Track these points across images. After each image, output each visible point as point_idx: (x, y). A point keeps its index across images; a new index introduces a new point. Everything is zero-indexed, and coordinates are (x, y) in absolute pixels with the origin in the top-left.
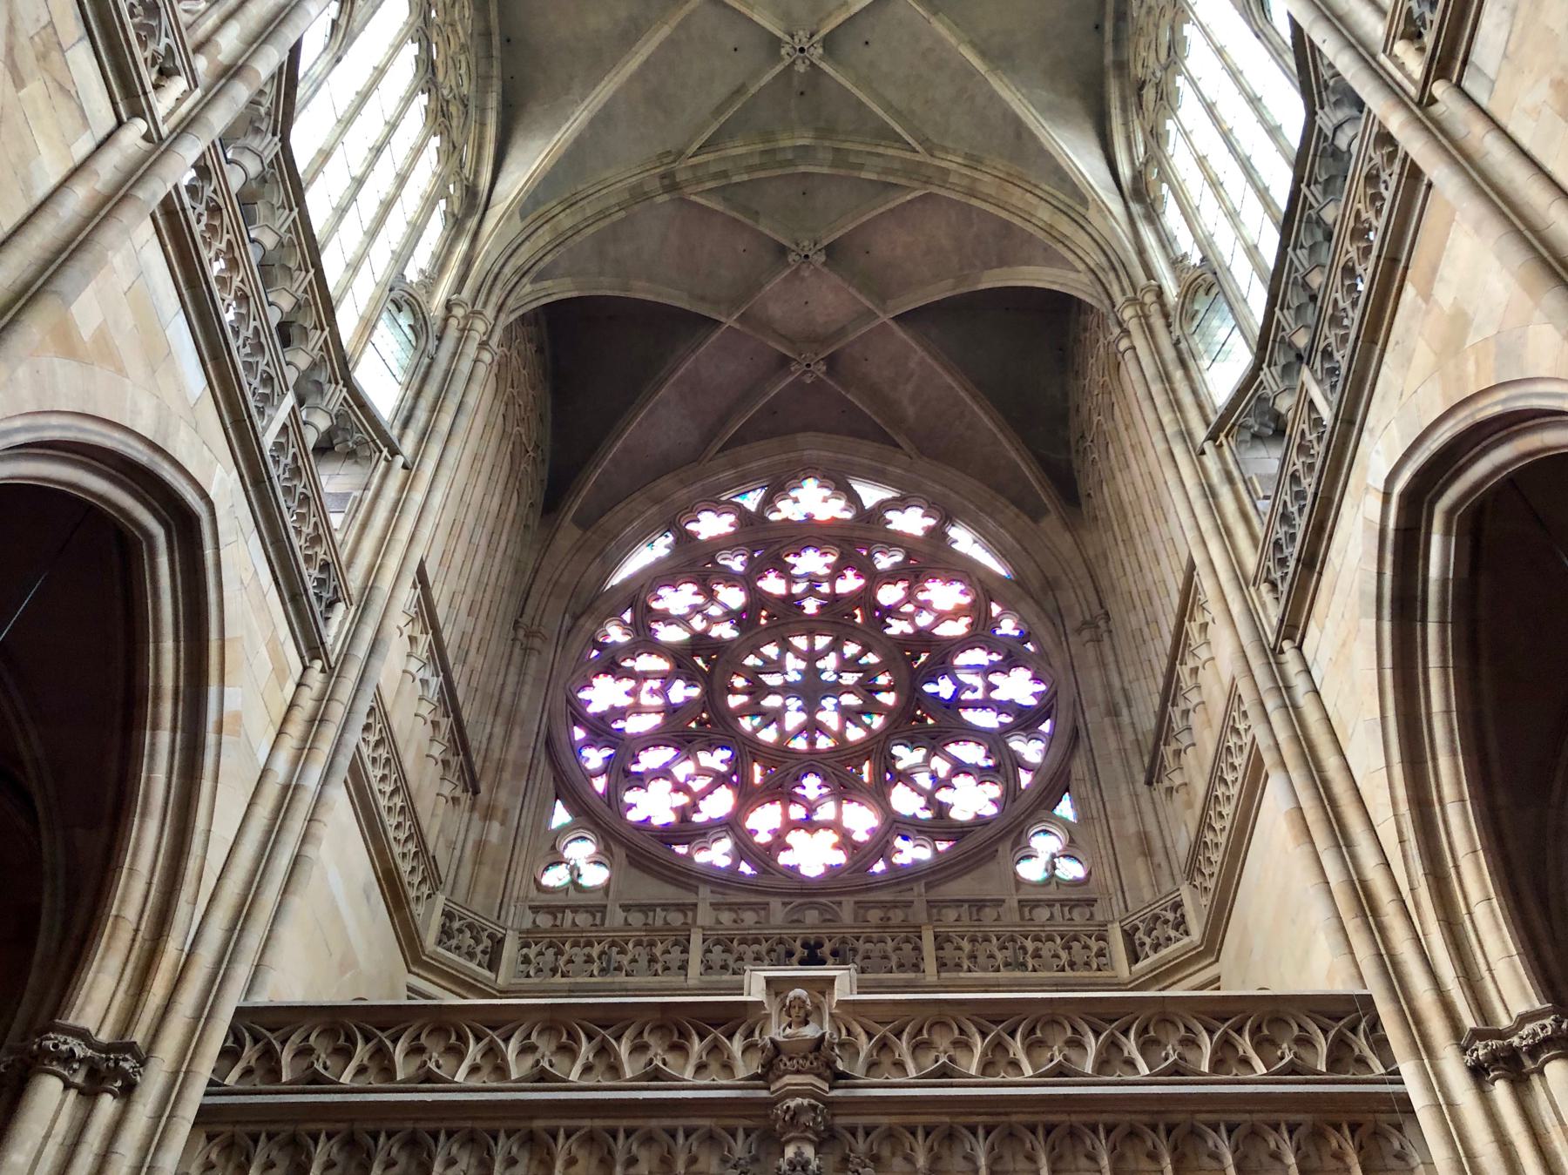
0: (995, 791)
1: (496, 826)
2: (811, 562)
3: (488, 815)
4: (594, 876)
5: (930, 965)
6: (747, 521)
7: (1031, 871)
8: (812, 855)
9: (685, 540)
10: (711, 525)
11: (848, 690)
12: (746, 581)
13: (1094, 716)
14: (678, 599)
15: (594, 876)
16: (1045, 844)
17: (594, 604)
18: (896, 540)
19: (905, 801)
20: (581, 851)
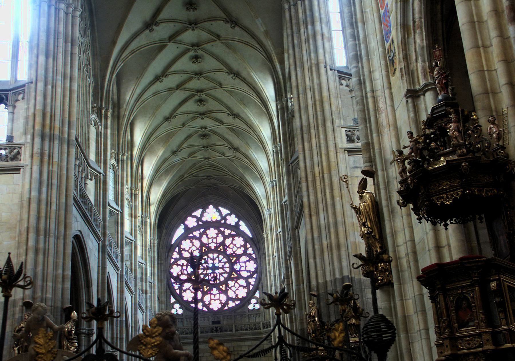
0: (246, 290)
1: (163, 305)
2: (212, 232)
3: (162, 303)
4: (180, 311)
5: (234, 330)
6: (199, 219)
7: (251, 307)
8: (215, 306)
9: (186, 228)
10: (191, 222)
11: (220, 268)
12: (199, 239)
13: (263, 275)
14: (186, 244)
15: (180, 311)
16: (253, 301)
17: (170, 249)
18: (229, 227)
19: (231, 294)
20: (177, 306)
